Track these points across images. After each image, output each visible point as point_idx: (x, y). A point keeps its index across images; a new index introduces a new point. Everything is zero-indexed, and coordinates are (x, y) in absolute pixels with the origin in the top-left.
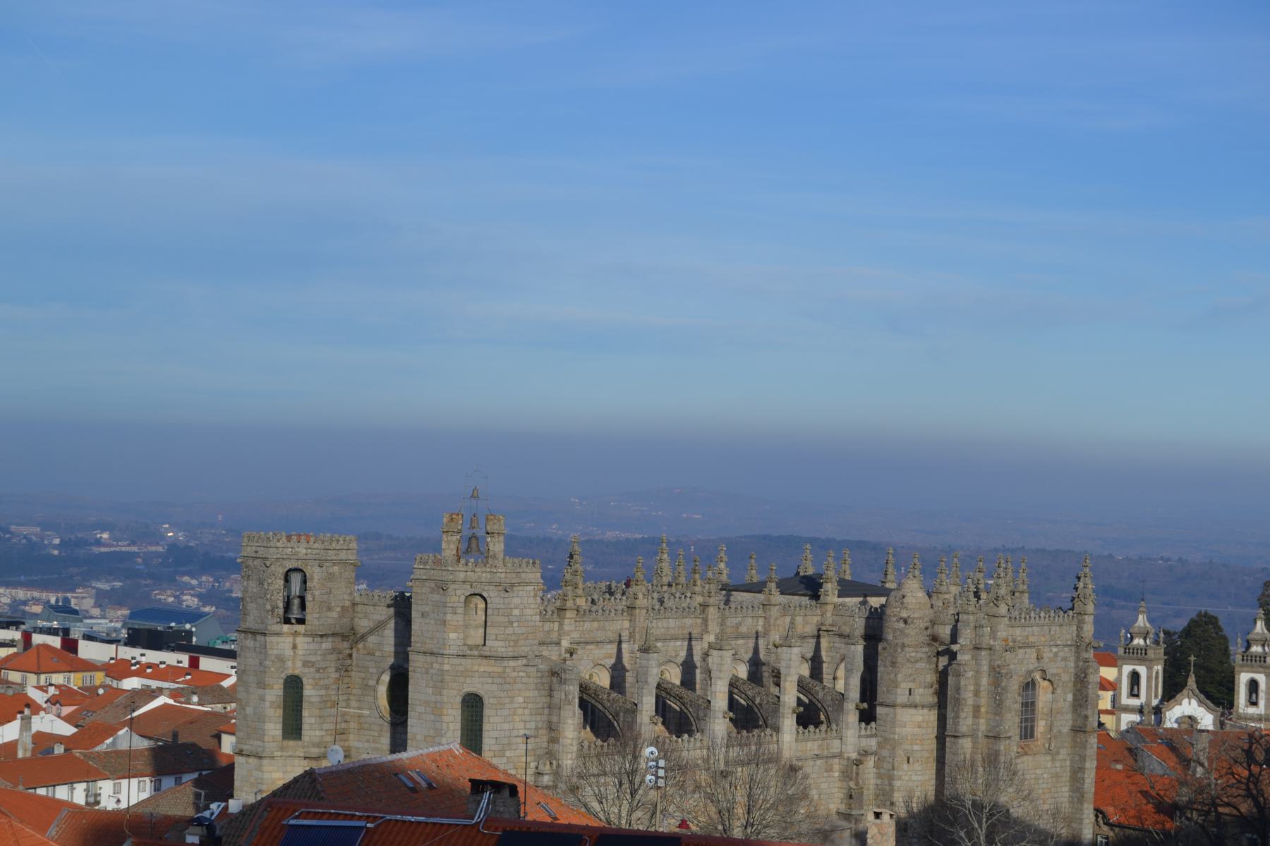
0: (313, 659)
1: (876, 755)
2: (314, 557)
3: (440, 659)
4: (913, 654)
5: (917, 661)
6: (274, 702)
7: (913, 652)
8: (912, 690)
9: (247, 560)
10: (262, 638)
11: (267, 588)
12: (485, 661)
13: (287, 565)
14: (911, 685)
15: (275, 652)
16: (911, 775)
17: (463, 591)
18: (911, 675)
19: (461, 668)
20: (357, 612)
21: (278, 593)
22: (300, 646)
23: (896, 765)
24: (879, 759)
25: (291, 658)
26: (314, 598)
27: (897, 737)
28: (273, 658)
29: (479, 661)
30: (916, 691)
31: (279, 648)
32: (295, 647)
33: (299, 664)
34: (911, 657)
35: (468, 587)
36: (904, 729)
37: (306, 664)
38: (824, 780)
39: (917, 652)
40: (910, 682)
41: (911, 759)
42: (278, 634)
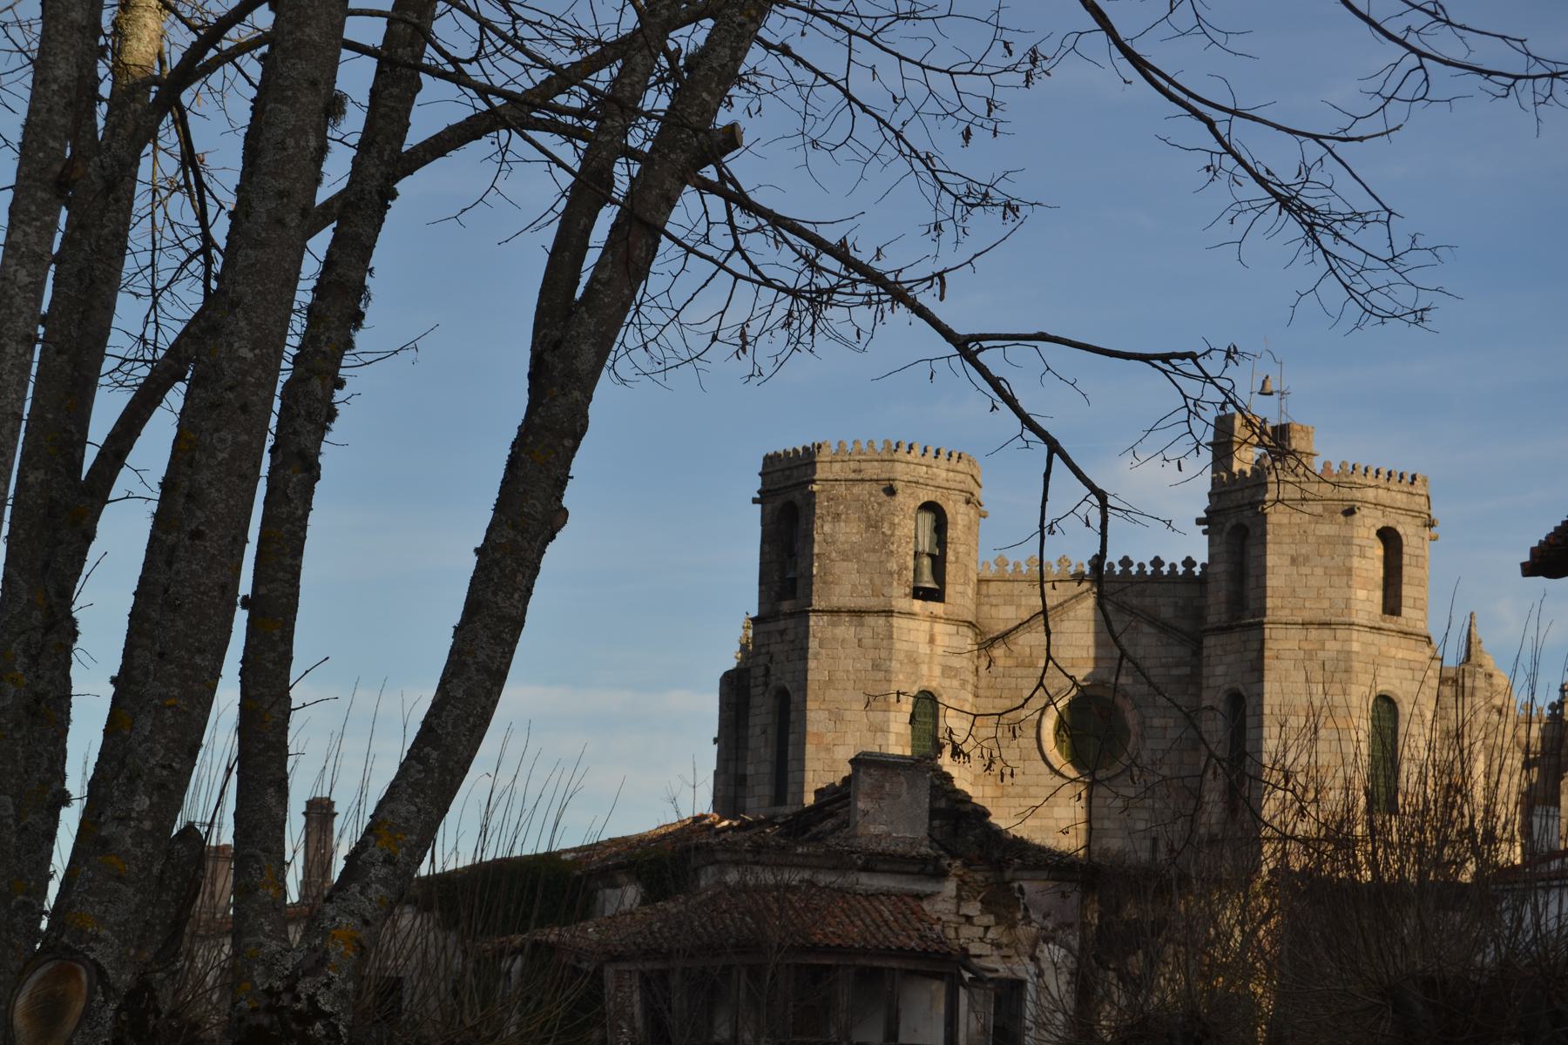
0: (956, 662)
2: (961, 486)
3: (1341, 633)
6: (902, 735)
9: (834, 486)
10: (881, 621)
11: (889, 533)
12: (1404, 642)
13: (921, 495)
15: (905, 646)
17: (1374, 521)
19: (1374, 650)
20: (988, 596)
21: (908, 543)
22: (939, 640)
25: (927, 660)
26: (957, 558)
28: (902, 656)
29: (1396, 640)
31: (912, 639)
32: (932, 641)
33: (937, 671)
35: (1380, 513)
37: (947, 671)
42: (911, 615)
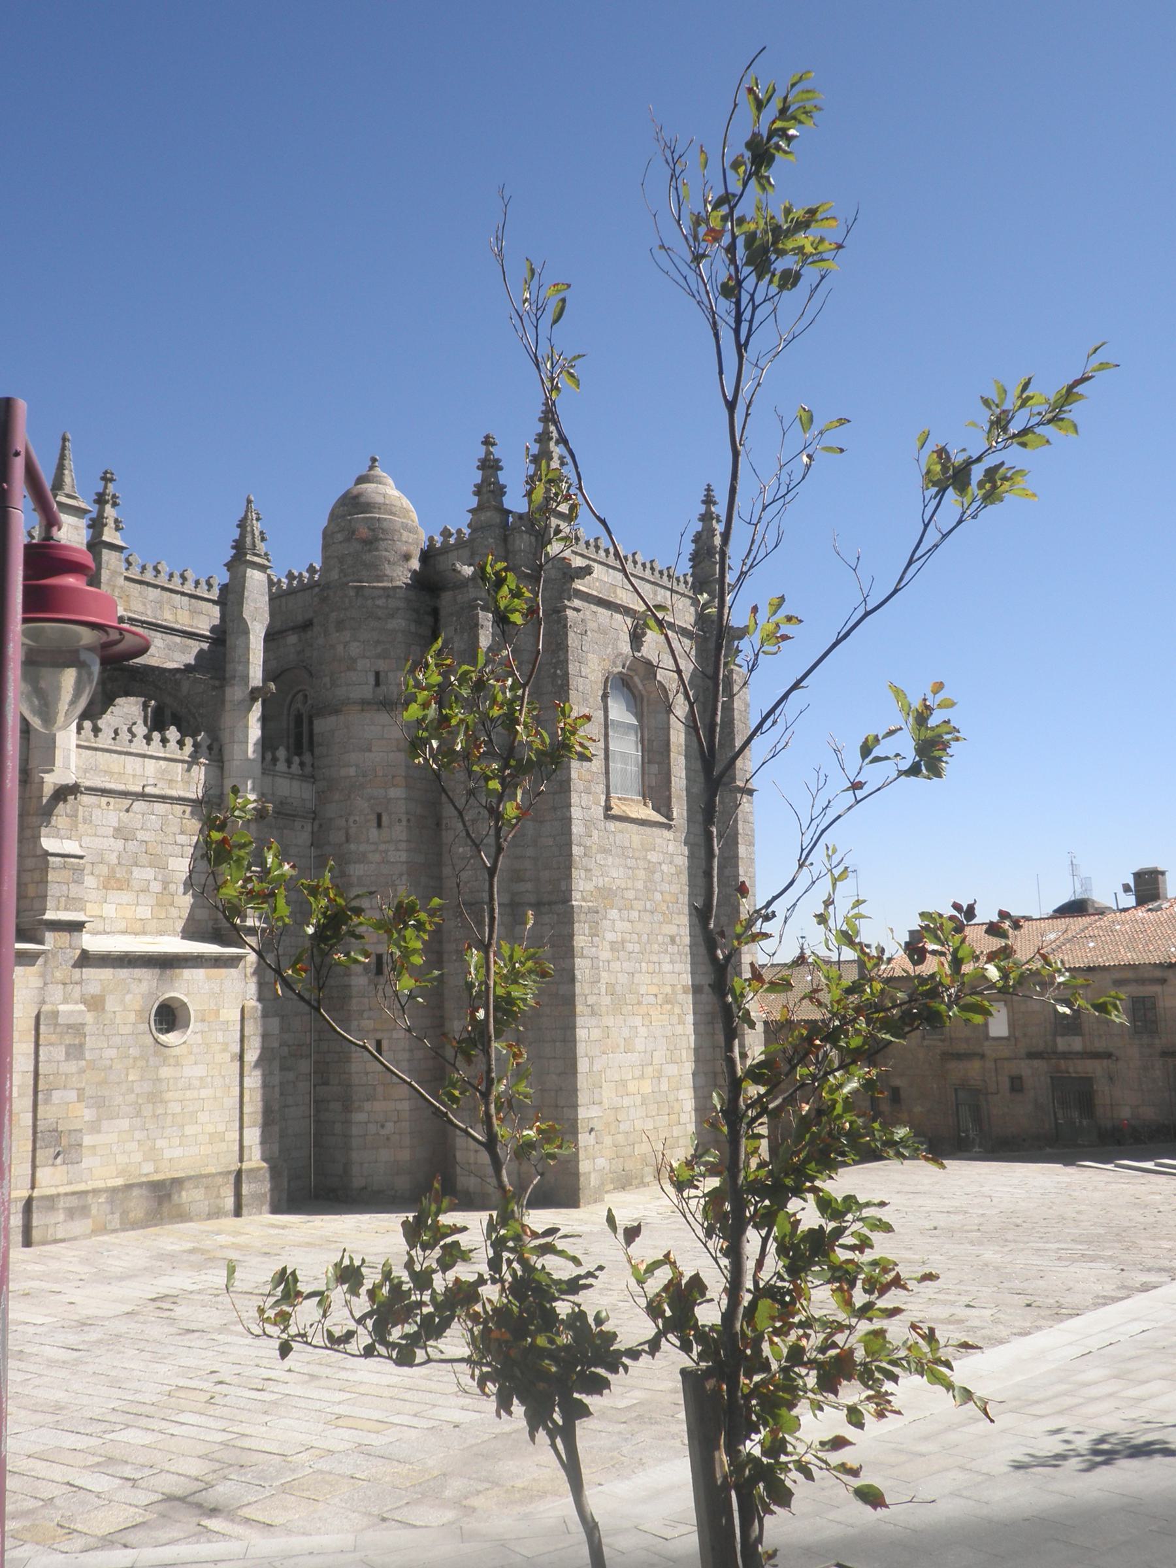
1: (314, 819)
4: (380, 602)
5: (392, 616)
7: (380, 597)
8: (382, 675)
14: (382, 665)
16: (386, 851)
18: (378, 642)
23: (353, 831)
24: (321, 826)
27: (352, 771)
30: (391, 675)
34: (378, 607)
36: (367, 754)
38: (177, 849)
39: (388, 596)
40: (378, 656)
41: (385, 818)
